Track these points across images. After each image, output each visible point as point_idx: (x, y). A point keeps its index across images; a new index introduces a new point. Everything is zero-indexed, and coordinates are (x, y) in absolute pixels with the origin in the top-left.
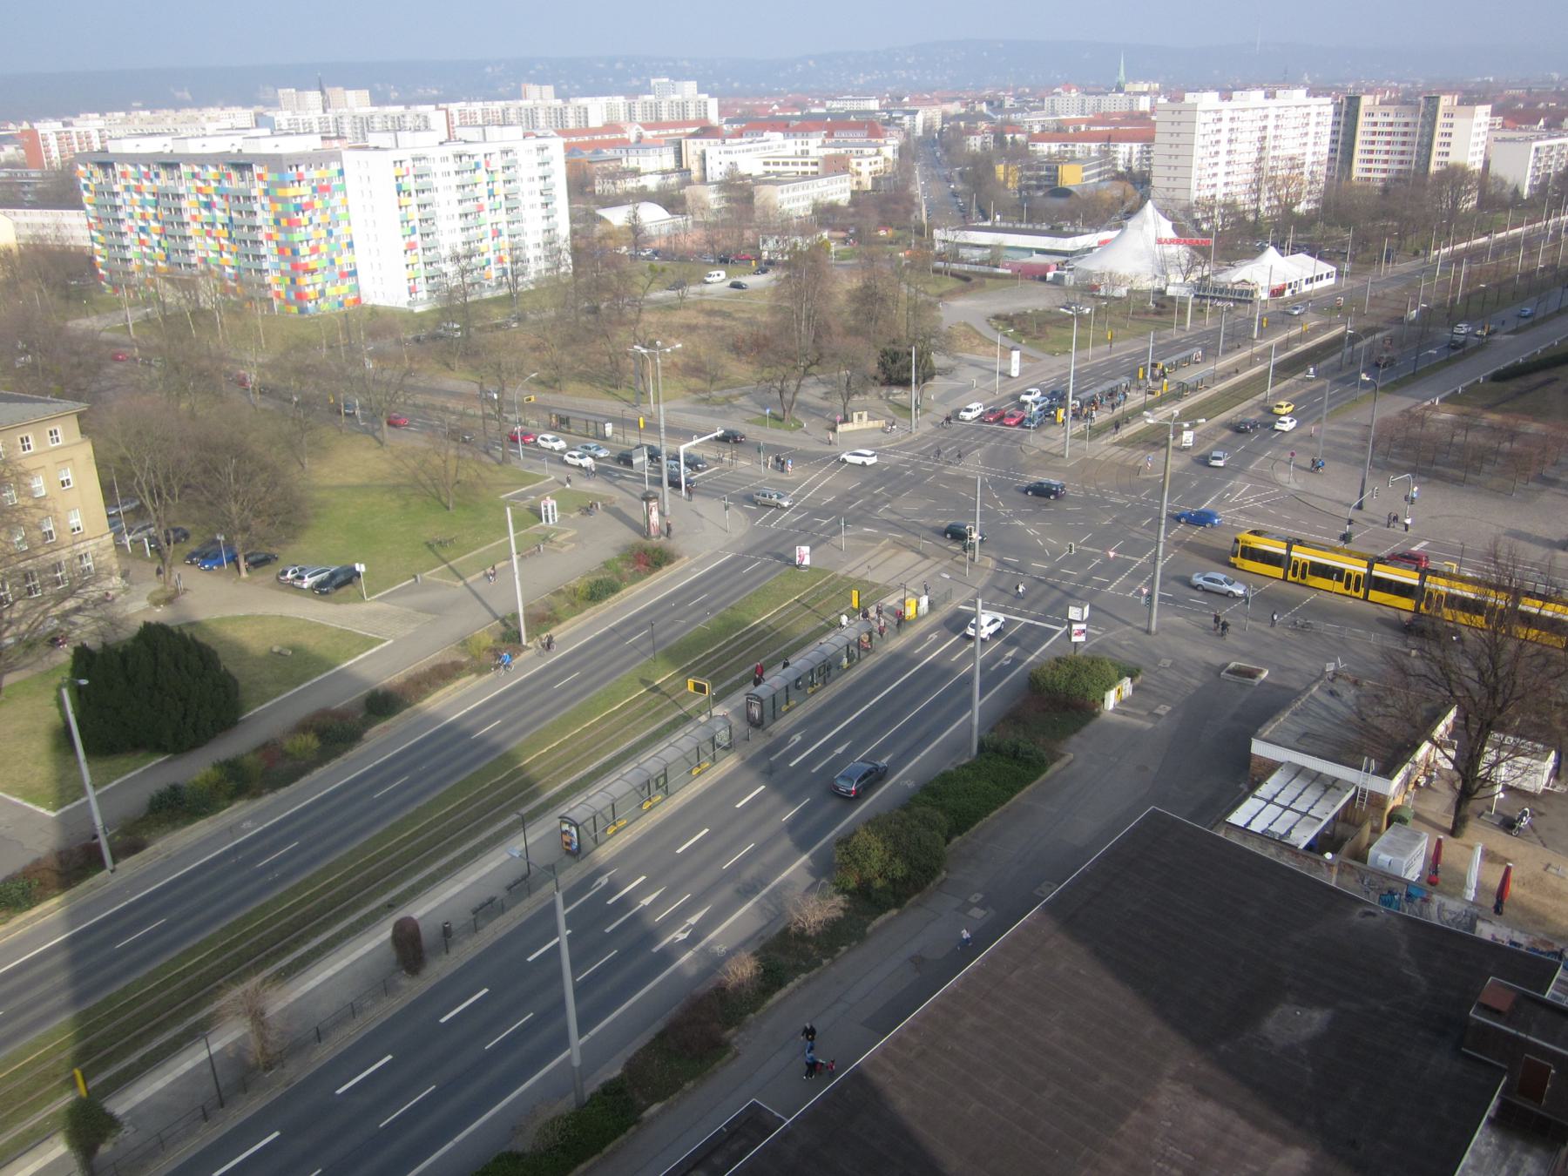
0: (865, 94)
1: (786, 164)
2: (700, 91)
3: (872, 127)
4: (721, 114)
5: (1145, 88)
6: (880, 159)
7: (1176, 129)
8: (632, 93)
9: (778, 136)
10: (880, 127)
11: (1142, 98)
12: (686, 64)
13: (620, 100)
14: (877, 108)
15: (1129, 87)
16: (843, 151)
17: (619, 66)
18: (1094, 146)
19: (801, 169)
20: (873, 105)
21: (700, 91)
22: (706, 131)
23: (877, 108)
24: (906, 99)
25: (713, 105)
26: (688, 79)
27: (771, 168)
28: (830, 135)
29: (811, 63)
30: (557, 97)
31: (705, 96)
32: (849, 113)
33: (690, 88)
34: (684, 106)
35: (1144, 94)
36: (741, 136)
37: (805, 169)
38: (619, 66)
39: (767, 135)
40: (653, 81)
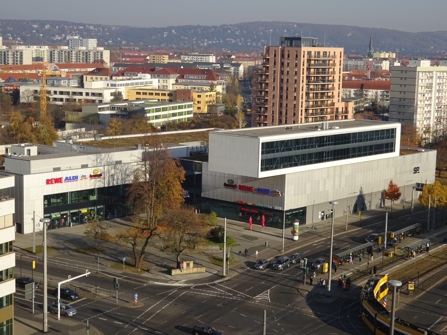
0: (207, 52)
1: (152, 94)
2: (98, 45)
3: (210, 74)
4: (111, 61)
5: (387, 56)
6: (213, 93)
7: (403, 82)
8: (53, 44)
9: (148, 76)
10: (214, 74)
11: (384, 62)
12: (91, 28)
13: (46, 49)
14: (214, 61)
15: (375, 55)
16: (189, 87)
17: (47, 27)
18: (352, 91)
19: (161, 97)
20: (212, 59)
21: (98, 45)
22: (100, 71)
23: (214, 61)
24: (233, 57)
25: (106, 56)
26: (92, 37)
27: (141, 96)
28: (182, 77)
29: (173, 31)
30: (3, 44)
31: (102, 49)
32: (196, 63)
33: (92, 43)
34: (87, 54)
35: (385, 59)
36: (123, 75)
37: (163, 98)
38: (47, 27)
39: (140, 75)
40: (68, 38)
